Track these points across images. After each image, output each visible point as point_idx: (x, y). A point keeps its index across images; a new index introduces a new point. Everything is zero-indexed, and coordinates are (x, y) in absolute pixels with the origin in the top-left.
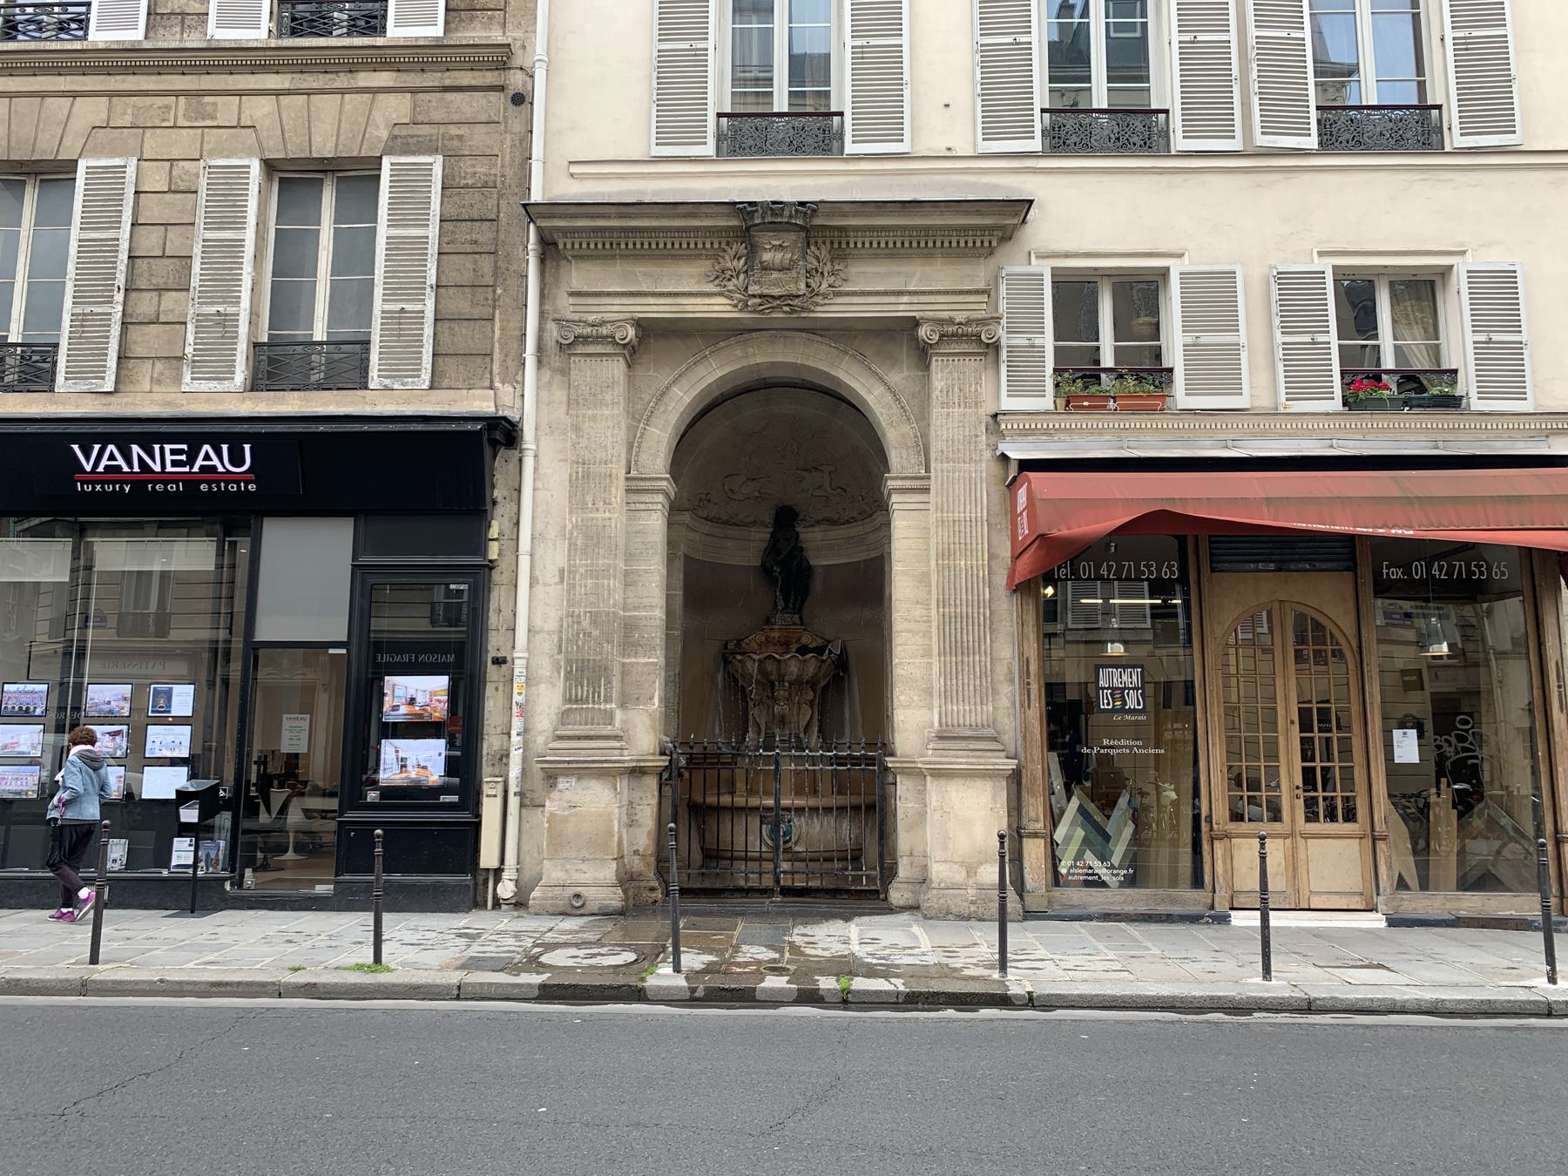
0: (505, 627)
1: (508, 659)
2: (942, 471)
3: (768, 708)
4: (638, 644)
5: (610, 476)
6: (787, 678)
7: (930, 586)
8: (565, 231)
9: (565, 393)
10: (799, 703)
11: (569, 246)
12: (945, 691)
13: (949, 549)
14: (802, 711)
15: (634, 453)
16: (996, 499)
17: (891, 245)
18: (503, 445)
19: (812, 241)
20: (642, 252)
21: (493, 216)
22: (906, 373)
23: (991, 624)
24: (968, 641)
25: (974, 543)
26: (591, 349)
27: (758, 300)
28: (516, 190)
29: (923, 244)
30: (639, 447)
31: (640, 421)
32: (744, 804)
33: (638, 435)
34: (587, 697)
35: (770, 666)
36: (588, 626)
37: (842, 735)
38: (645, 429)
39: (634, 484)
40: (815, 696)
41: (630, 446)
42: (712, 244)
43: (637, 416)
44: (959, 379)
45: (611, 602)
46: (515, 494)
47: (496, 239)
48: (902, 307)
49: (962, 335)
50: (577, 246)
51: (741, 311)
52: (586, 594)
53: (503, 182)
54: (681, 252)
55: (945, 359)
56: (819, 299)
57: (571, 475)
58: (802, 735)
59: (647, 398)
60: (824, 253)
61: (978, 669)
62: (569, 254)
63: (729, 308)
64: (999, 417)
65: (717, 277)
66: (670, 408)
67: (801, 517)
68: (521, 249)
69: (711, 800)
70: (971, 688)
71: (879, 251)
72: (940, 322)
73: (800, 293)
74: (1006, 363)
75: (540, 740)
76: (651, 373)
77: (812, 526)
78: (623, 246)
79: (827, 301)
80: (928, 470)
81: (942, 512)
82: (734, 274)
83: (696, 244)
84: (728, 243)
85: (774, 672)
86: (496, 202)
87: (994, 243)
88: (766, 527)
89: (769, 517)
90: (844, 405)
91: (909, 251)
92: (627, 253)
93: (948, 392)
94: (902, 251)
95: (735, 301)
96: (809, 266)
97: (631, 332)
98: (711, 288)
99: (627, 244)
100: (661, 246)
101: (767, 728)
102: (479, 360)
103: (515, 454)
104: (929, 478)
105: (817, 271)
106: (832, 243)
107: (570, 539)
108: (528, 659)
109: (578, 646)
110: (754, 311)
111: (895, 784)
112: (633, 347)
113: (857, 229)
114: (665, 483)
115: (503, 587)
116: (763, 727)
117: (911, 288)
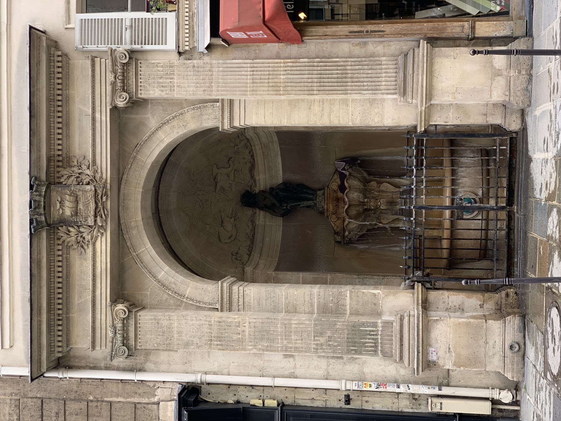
0: (324, 396)
1: (346, 393)
2: (218, 91)
3: (382, 213)
4: (337, 305)
5: (220, 322)
6: (361, 200)
7: (298, 100)
8: (50, 352)
9: (162, 353)
10: (379, 192)
11: (60, 349)
12: (372, 90)
13: (273, 86)
15: (204, 306)
16: (237, 53)
17: (60, 126)
18: (198, 396)
19: (57, 180)
20: (64, 298)
21: (39, 402)
22: (149, 116)
23: (325, 57)
24: (337, 74)
25: (268, 69)
26: (132, 334)
27: (98, 218)
28: (21, 385)
29: (60, 103)
30: (200, 302)
31: (182, 301)
32: (449, 231)
33: (191, 302)
34: (373, 339)
35: (353, 212)
36: (325, 339)
37: (401, 162)
38: (187, 298)
39: (226, 306)
40: (374, 180)
41: (199, 308)
42: (59, 250)
43: (178, 303)
44: (154, 78)
45: (308, 322)
46: (231, 387)
47: (55, 400)
48: (104, 118)
49: (123, 76)
50: (60, 344)
51: (105, 230)
52: (302, 340)
53: (16, 395)
54: (65, 272)
55: (140, 88)
56: (98, 176)
57: (220, 350)
58: (401, 190)
59: (166, 296)
60: (65, 172)
61: (357, 67)
62: (65, 349)
63: (104, 239)
64: (181, 50)
65: (82, 247)
66: (173, 280)
67: (249, 189)
68: (61, 382)
69: (445, 253)
70: (370, 72)
71: (65, 133)
72: (114, 91)
73: (93, 189)
74: (143, 46)
75: (403, 372)
76: (148, 293)
77: (255, 181)
78: (60, 312)
79: (99, 171)
80: (217, 101)
81: (247, 91)
82: (80, 235)
83: (59, 261)
84: (59, 239)
85: (357, 208)
86: (30, 399)
87: (59, 53)
88: (255, 213)
89: (249, 212)
90: (171, 158)
91: (64, 112)
92: (65, 309)
93: (163, 86)
94: (64, 117)
95: (99, 234)
96: (75, 183)
97: (120, 307)
98: (90, 251)
99: (59, 309)
100: (60, 285)
101: (396, 214)
102: (138, 412)
103: (204, 388)
104: (223, 100)
105: (78, 177)
106: (58, 166)
107: (263, 350)
108: (347, 380)
109: (338, 345)
110: (106, 221)
111: (436, 125)
112: (131, 305)
113: (49, 149)
114: (225, 284)
115: (297, 397)
116: (396, 217)
117: (90, 111)
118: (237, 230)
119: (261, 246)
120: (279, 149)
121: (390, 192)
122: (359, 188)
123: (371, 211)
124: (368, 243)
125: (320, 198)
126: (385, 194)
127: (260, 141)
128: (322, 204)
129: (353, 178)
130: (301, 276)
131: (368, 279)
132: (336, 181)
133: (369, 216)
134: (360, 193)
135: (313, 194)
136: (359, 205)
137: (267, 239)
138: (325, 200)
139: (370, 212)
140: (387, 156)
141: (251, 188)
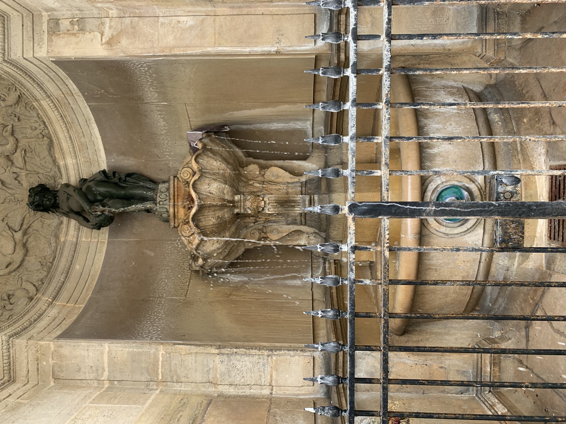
3: (269, 222)
6: (227, 197)
10: (263, 183)
14: (273, 179)
35: (210, 220)
37: (302, 133)
40: (254, 163)
58: (303, 179)
85: (219, 213)
88: (62, 222)
101: (294, 223)
116: (296, 228)
118: (27, 251)
119: (62, 279)
120: (88, 109)
121: (283, 184)
122: (223, 176)
123: (249, 217)
125: (163, 196)
126: (274, 187)
128: (166, 207)
129: (211, 155)
130: (107, 349)
131: (238, 357)
132: (190, 165)
133: (246, 227)
134: (226, 184)
135: (153, 190)
136: (223, 207)
137: (78, 267)
138: (170, 199)
139: (248, 220)
140: (279, 121)
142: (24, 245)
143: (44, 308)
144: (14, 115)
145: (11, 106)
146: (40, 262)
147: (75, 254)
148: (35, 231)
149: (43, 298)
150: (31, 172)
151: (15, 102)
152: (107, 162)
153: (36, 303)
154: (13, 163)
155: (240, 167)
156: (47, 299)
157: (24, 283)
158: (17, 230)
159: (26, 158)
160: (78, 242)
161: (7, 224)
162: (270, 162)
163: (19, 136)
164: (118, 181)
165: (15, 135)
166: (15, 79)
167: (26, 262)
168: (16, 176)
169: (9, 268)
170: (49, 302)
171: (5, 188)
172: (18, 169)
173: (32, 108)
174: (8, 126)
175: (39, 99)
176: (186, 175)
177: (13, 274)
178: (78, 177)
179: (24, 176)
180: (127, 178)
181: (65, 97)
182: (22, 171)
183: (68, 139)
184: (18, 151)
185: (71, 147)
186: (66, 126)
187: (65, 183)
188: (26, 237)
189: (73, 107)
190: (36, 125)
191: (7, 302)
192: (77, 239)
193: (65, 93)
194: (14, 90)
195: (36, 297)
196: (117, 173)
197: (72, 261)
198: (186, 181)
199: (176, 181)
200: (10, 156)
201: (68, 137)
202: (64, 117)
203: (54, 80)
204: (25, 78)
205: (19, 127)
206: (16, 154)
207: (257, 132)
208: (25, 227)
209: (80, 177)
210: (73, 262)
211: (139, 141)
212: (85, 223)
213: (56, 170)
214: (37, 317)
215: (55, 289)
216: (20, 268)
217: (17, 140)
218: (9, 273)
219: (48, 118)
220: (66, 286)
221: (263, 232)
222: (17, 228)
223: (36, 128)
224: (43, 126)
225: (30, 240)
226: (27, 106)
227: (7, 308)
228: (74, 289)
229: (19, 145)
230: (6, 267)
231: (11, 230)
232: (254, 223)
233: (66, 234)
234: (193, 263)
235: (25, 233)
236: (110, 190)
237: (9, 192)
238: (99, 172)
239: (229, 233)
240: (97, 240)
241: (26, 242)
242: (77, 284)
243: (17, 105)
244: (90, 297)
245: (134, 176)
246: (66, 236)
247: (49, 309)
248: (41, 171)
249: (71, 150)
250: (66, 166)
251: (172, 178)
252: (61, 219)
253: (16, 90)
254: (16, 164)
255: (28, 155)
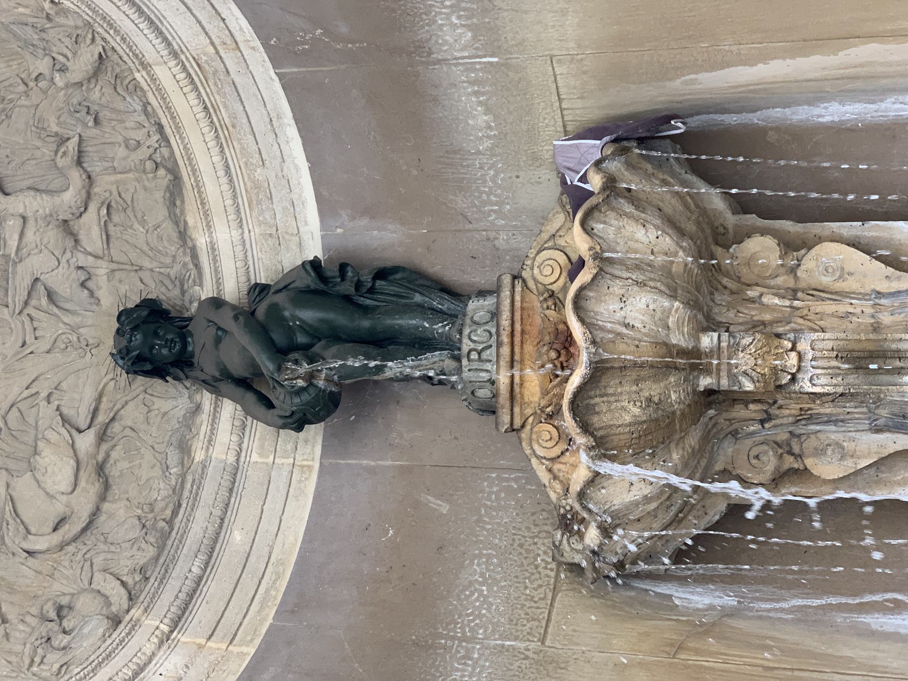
3: (812, 419)
6: (678, 339)
10: (793, 293)
14: (826, 280)
40: (763, 232)
85: (653, 389)
88: (198, 408)
118: (107, 486)
119: (196, 570)
121: (864, 296)
122: (666, 271)
123: (746, 403)
124: (734, 580)
125: (480, 334)
126: (829, 307)
127: (160, 33)
128: (488, 366)
129: (629, 208)
132: (561, 242)
133: (735, 434)
134: (674, 297)
135: (451, 317)
136: (661, 370)
138: (499, 344)
139: (739, 412)
141: (183, 292)
142: (101, 469)
143: (149, 649)
144: (86, 110)
145: (80, 84)
146: (139, 518)
147: (233, 500)
148: (128, 432)
149: (147, 622)
150: (121, 267)
151: (91, 72)
152: (323, 237)
153: (128, 634)
154: (77, 241)
155: (717, 244)
156: (157, 623)
157: (98, 576)
158: (83, 427)
159: (111, 228)
160: (241, 464)
161: (58, 409)
162: (816, 228)
163: (95, 166)
164: (352, 290)
165: (85, 165)
166: (94, 11)
167: (103, 518)
168: (83, 278)
169: (61, 531)
170: (163, 633)
171: (56, 310)
172: (90, 259)
173: (131, 87)
174: (68, 139)
175: (151, 61)
176: (547, 271)
177: (71, 549)
178: (243, 279)
179: (105, 277)
180: (379, 283)
181: (217, 52)
182: (100, 262)
183: (221, 173)
184: (92, 208)
185: (228, 194)
186: (217, 137)
187: (211, 295)
188: (104, 447)
189: (238, 80)
190: (139, 135)
191: (56, 628)
192: (239, 455)
193: (217, 42)
194: (88, 41)
195: (128, 618)
196: (349, 268)
197: (222, 520)
198: (548, 290)
199: (518, 289)
200: (71, 223)
201: (220, 166)
202: (211, 111)
203: (191, 7)
204: (118, 7)
205: (95, 142)
206: (85, 217)
207: (771, 133)
208: (102, 418)
209: (249, 280)
210: (226, 521)
211: (415, 172)
212: (261, 410)
213: (188, 259)
214: (130, 673)
215: (177, 597)
216: (89, 533)
217: (89, 177)
218: (61, 547)
219: (172, 114)
220: (205, 589)
221: (790, 453)
222: (83, 423)
223: (138, 142)
224: (157, 137)
225: (114, 455)
226: (118, 81)
227: (55, 643)
228: (226, 599)
229: (96, 190)
230: (55, 530)
231: (67, 426)
232: (762, 422)
233: (210, 441)
234: (565, 541)
235: (102, 437)
236: (330, 316)
237: (65, 320)
238: (303, 264)
239: (681, 452)
240: (292, 461)
241: (105, 461)
242: (236, 585)
243: (93, 81)
244: (271, 625)
245: (398, 276)
246: (208, 448)
247: (162, 652)
248: (147, 264)
249: (229, 202)
250: (213, 249)
251: (507, 280)
252: (198, 397)
253: (93, 39)
254: (85, 243)
255: (116, 218)
